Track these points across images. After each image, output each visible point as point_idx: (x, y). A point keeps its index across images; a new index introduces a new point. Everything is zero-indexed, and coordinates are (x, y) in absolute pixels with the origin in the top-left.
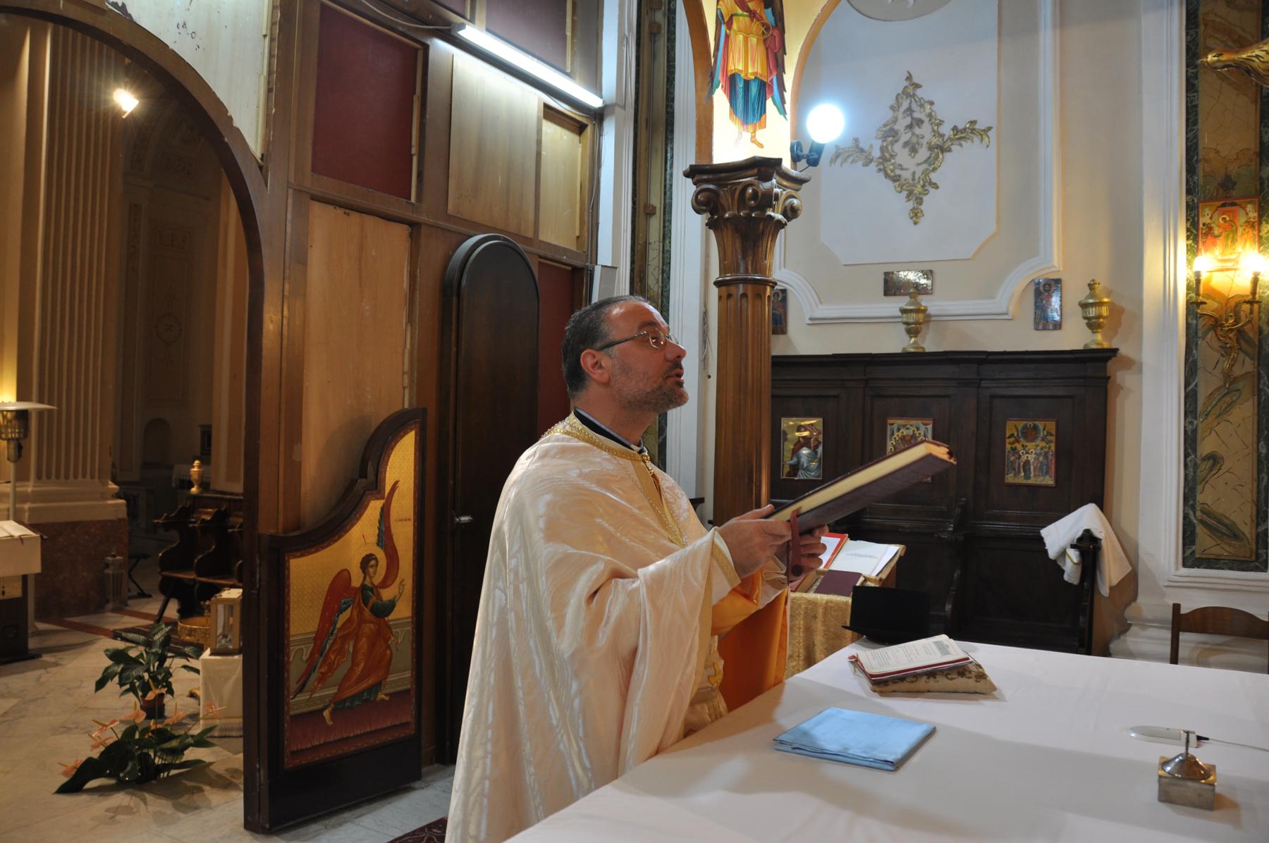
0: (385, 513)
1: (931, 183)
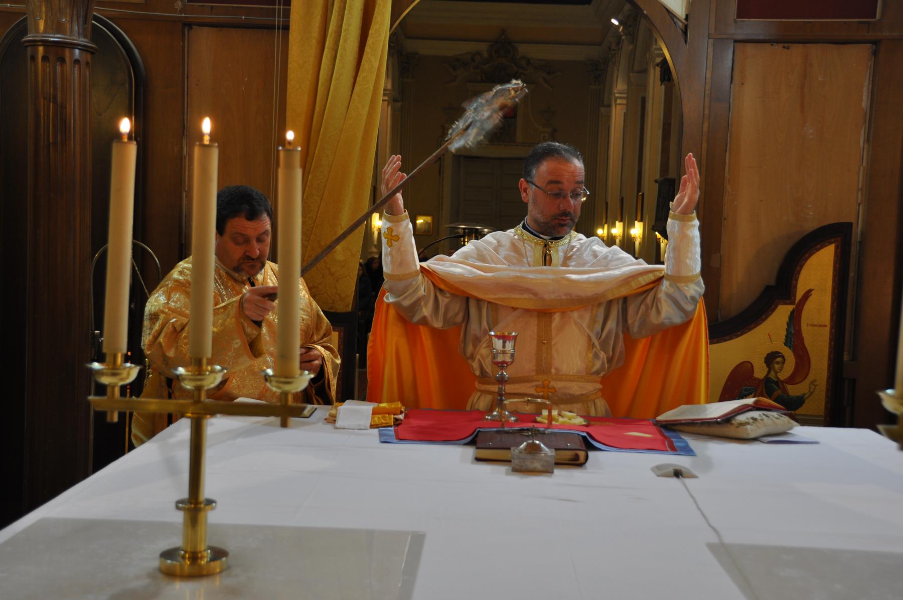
0: (795, 319)
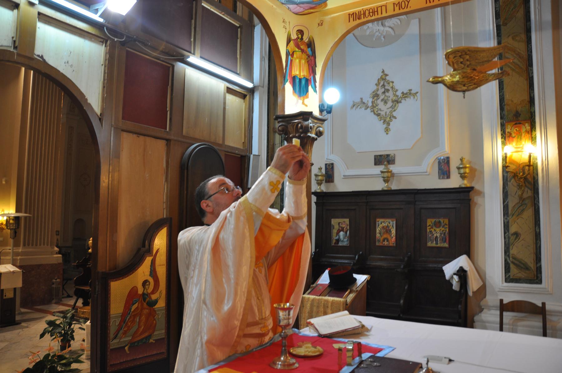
0: (153, 263)
1: (393, 117)
